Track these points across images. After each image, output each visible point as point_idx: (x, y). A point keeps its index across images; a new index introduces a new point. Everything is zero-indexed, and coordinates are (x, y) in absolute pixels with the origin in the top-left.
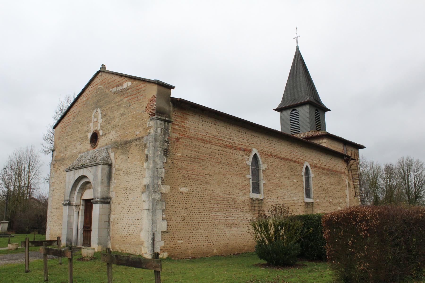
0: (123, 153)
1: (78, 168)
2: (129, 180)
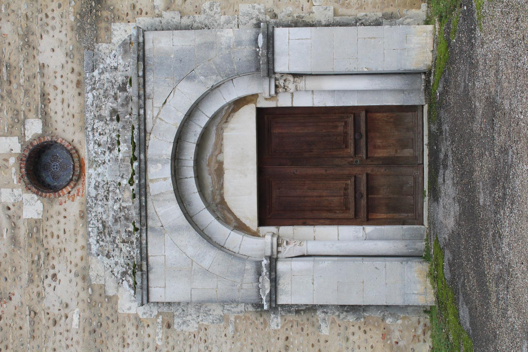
1: (143, 198)
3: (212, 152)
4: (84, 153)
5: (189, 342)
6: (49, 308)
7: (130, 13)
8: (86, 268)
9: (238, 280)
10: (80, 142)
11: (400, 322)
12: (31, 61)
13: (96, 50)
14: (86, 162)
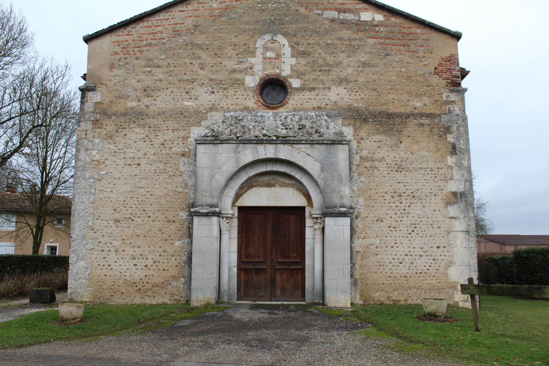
0: (383, 133)
1: (255, 142)
2: (408, 181)
3: (280, 181)
4: (281, 110)
5: (173, 166)
6: (195, 89)
7: (359, 137)
8: (217, 110)
9: (208, 194)
10: (287, 108)
11: (182, 286)
12: (332, 83)
13: (338, 118)
14: (276, 111)
